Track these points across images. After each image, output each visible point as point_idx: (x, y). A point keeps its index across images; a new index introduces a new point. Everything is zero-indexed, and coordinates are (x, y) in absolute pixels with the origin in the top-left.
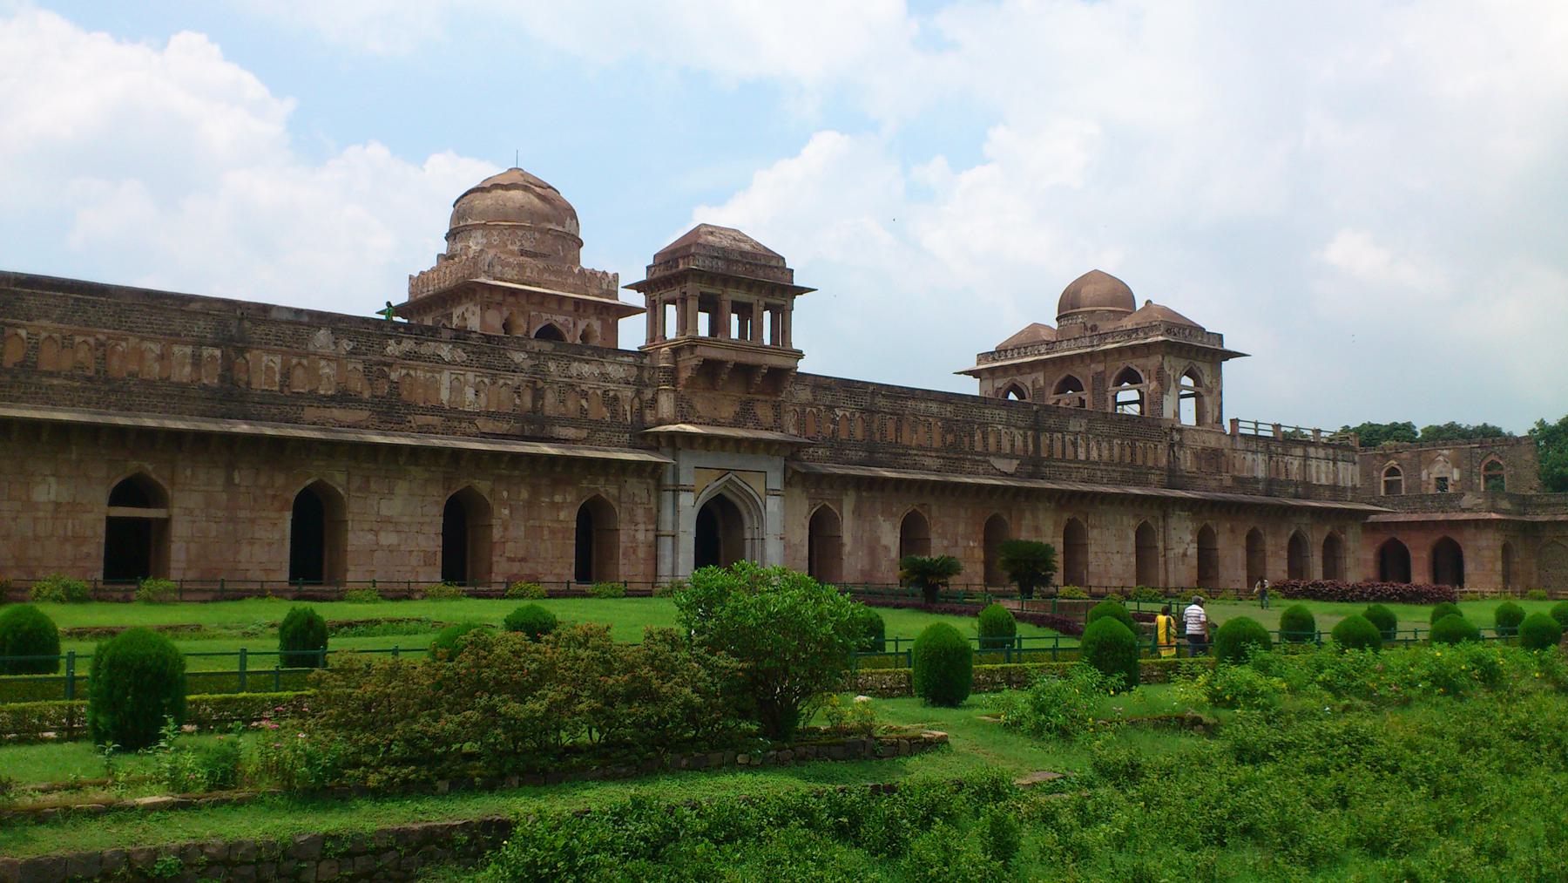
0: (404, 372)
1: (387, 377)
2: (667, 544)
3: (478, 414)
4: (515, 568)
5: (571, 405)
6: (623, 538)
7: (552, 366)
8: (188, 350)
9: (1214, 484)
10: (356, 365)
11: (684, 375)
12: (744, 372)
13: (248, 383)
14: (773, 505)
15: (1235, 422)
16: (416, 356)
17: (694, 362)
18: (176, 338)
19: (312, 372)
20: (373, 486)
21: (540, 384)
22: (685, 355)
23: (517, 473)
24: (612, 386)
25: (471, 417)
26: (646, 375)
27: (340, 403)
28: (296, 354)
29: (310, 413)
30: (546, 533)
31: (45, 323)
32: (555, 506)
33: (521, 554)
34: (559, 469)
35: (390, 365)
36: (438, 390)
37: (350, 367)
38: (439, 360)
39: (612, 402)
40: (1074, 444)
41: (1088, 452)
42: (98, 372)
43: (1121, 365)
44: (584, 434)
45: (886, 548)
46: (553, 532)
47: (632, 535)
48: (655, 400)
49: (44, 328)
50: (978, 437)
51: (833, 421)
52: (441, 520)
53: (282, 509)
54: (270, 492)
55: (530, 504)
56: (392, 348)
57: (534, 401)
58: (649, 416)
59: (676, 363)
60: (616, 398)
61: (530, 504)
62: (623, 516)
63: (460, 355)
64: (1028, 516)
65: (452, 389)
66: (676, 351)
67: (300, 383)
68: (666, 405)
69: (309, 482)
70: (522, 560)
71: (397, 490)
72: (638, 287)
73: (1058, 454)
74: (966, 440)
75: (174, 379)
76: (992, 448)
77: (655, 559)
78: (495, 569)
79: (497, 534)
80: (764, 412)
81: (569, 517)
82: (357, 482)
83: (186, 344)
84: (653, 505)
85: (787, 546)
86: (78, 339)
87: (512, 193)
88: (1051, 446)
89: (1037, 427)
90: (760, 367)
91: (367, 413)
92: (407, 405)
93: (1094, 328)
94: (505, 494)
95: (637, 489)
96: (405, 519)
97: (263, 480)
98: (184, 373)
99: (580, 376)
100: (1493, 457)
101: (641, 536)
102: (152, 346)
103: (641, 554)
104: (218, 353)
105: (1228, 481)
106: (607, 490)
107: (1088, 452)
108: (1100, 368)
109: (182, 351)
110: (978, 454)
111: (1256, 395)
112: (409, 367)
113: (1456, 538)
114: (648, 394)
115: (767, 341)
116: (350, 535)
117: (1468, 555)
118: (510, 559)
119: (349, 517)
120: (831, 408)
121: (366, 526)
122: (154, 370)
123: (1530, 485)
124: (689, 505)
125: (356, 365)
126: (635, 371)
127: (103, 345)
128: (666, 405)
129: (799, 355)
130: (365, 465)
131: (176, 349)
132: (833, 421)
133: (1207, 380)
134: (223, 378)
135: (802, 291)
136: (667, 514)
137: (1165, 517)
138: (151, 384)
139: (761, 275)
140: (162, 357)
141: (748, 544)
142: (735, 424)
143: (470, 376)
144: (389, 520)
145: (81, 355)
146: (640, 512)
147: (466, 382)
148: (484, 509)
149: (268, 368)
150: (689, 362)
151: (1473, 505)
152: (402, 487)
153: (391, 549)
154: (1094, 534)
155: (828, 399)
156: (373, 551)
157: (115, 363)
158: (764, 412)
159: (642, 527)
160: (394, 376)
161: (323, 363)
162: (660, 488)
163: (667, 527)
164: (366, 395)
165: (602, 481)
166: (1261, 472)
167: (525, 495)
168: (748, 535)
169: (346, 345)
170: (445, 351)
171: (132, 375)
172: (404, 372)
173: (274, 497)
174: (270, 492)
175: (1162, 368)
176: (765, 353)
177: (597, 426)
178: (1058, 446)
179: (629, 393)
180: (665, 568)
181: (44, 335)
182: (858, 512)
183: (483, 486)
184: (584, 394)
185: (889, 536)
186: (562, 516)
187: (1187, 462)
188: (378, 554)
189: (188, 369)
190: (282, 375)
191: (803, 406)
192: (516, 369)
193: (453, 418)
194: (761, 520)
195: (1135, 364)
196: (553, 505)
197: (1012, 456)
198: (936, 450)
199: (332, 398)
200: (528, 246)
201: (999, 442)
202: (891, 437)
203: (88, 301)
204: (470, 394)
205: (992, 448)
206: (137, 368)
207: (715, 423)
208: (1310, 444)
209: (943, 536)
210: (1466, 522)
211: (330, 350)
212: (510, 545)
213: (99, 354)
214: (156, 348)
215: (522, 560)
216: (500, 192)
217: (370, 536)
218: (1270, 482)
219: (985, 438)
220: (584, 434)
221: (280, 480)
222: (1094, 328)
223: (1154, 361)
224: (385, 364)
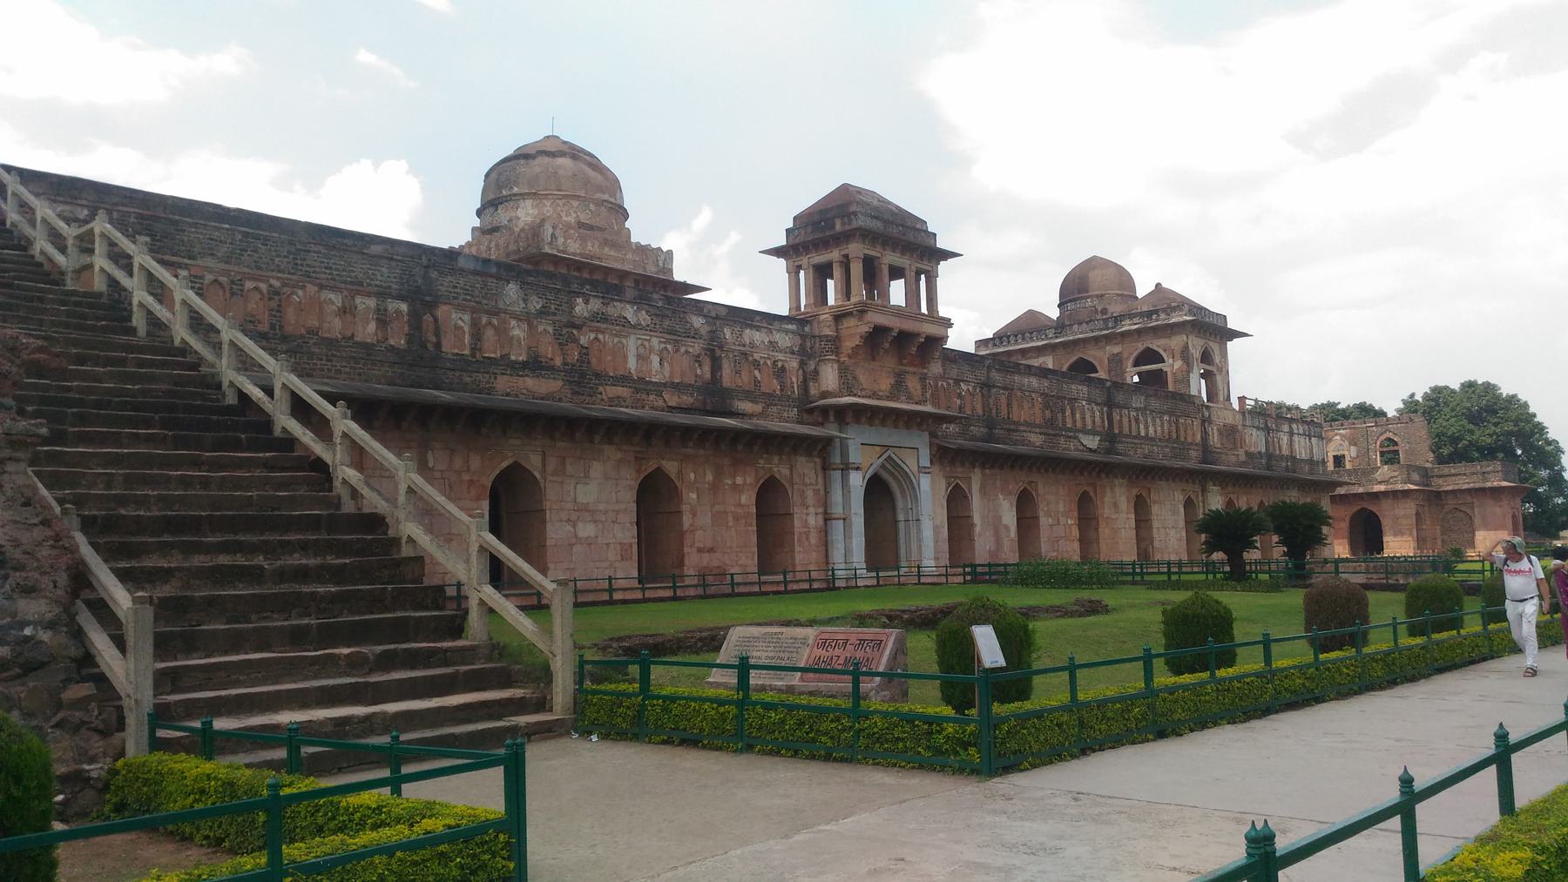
0: (592, 336)
1: (576, 341)
2: (838, 527)
3: (665, 385)
4: (706, 559)
5: (745, 376)
6: (797, 523)
7: (727, 332)
8: (372, 303)
9: (1233, 459)
10: (545, 326)
11: (848, 345)
12: (904, 338)
13: (438, 345)
14: (925, 483)
15: (1242, 399)
16: (605, 318)
17: (865, 329)
18: (357, 287)
19: (502, 331)
20: (569, 469)
21: (718, 352)
22: (850, 322)
23: (702, 452)
24: (781, 356)
25: (658, 388)
26: (808, 344)
27: (533, 371)
28: (488, 313)
29: (503, 383)
30: (730, 518)
31: (210, 262)
32: (736, 488)
33: (709, 544)
34: (740, 447)
35: (579, 327)
36: (625, 357)
37: (541, 328)
38: (625, 322)
39: (780, 372)
40: (1137, 420)
41: (1147, 428)
42: (272, 327)
44: (758, 408)
45: (1006, 527)
46: (736, 519)
47: (806, 519)
48: (816, 372)
49: (211, 271)
50: (1068, 413)
51: (959, 396)
52: (634, 506)
53: (478, 499)
54: (466, 477)
55: (715, 487)
56: (581, 308)
57: (713, 372)
58: (813, 391)
59: (837, 330)
60: (783, 369)
61: (715, 487)
62: (796, 498)
63: (645, 318)
64: (1108, 493)
65: (639, 357)
66: (839, 317)
67: (491, 350)
68: (829, 377)
69: (505, 464)
70: (711, 550)
71: (593, 473)
72: (777, 252)
73: (1126, 431)
74: (1060, 416)
75: (357, 339)
76: (1079, 425)
77: (826, 545)
78: (686, 562)
79: (687, 520)
80: (913, 384)
81: (748, 499)
82: (552, 464)
83: (369, 295)
84: (820, 486)
85: (936, 529)
86: (249, 285)
87: (560, 161)
88: (1120, 422)
89: (1110, 404)
90: (918, 335)
91: (560, 383)
92: (597, 375)
93: (1104, 311)
94: (692, 476)
95: (806, 468)
96: (601, 507)
97: (458, 463)
98: (368, 331)
99: (752, 345)
100: (1391, 435)
101: (812, 521)
102: (332, 296)
103: (813, 541)
104: (404, 307)
105: (1243, 458)
106: (781, 470)
107: (1147, 428)
108: (1116, 349)
109: (365, 303)
110: (1070, 430)
111: (1259, 373)
112: (598, 330)
113: (1374, 509)
114: (812, 365)
115: (924, 310)
116: (549, 526)
117: (1386, 523)
118: (700, 550)
119: (547, 505)
120: (957, 382)
121: (564, 516)
122: (335, 327)
123: (1427, 459)
124: (857, 481)
125: (545, 326)
126: (798, 340)
127: (278, 293)
128: (829, 377)
129: (947, 323)
130: (560, 444)
131: (358, 300)
132: (959, 396)
133: (1217, 359)
134: (410, 339)
135: (947, 255)
136: (837, 496)
137: (1204, 491)
138: (331, 343)
139: (910, 237)
140: (346, 311)
141: (902, 526)
142: (888, 398)
143: (655, 341)
144: (583, 509)
145: (251, 306)
146: (810, 493)
147: (651, 350)
148: (674, 493)
149: (457, 328)
150: (855, 330)
152: (597, 469)
153: (589, 543)
154: (1155, 509)
155: (954, 373)
156: (571, 545)
157: (290, 315)
159: (812, 510)
160: (583, 341)
161: (513, 323)
162: (826, 468)
163: (838, 510)
164: (558, 362)
165: (776, 459)
167: (709, 477)
168: (901, 517)
169: (536, 304)
170: (629, 312)
171: (313, 332)
172: (592, 336)
173: (471, 482)
174: (466, 477)
175: (1186, 347)
176: (923, 321)
177: (769, 399)
178: (1125, 420)
179: (793, 364)
180: (837, 556)
181: (209, 278)
182: (983, 489)
183: (671, 467)
184: (756, 364)
185: (1009, 517)
186: (744, 499)
187: (1215, 439)
188: (577, 548)
189: (372, 327)
190: (472, 335)
191: (936, 379)
192: (695, 335)
193: (641, 385)
194: (916, 498)
195: (1157, 344)
196: (735, 486)
197: (1093, 433)
198: (1039, 426)
199: (525, 365)
200: (584, 218)
201: (1083, 418)
202: (1004, 413)
203: (257, 238)
204: (655, 360)
205: (1079, 425)
206: (317, 324)
207: (874, 395)
208: (1292, 420)
209: (1048, 514)
210: (1385, 494)
211: (519, 307)
212: (699, 532)
213: (273, 304)
214: (336, 299)
215: (711, 550)
216: (547, 159)
217: (569, 528)
219: (1073, 414)
220: (758, 408)
221: (476, 462)
222: (1104, 311)
223: (1177, 341)
224: (574, 326)
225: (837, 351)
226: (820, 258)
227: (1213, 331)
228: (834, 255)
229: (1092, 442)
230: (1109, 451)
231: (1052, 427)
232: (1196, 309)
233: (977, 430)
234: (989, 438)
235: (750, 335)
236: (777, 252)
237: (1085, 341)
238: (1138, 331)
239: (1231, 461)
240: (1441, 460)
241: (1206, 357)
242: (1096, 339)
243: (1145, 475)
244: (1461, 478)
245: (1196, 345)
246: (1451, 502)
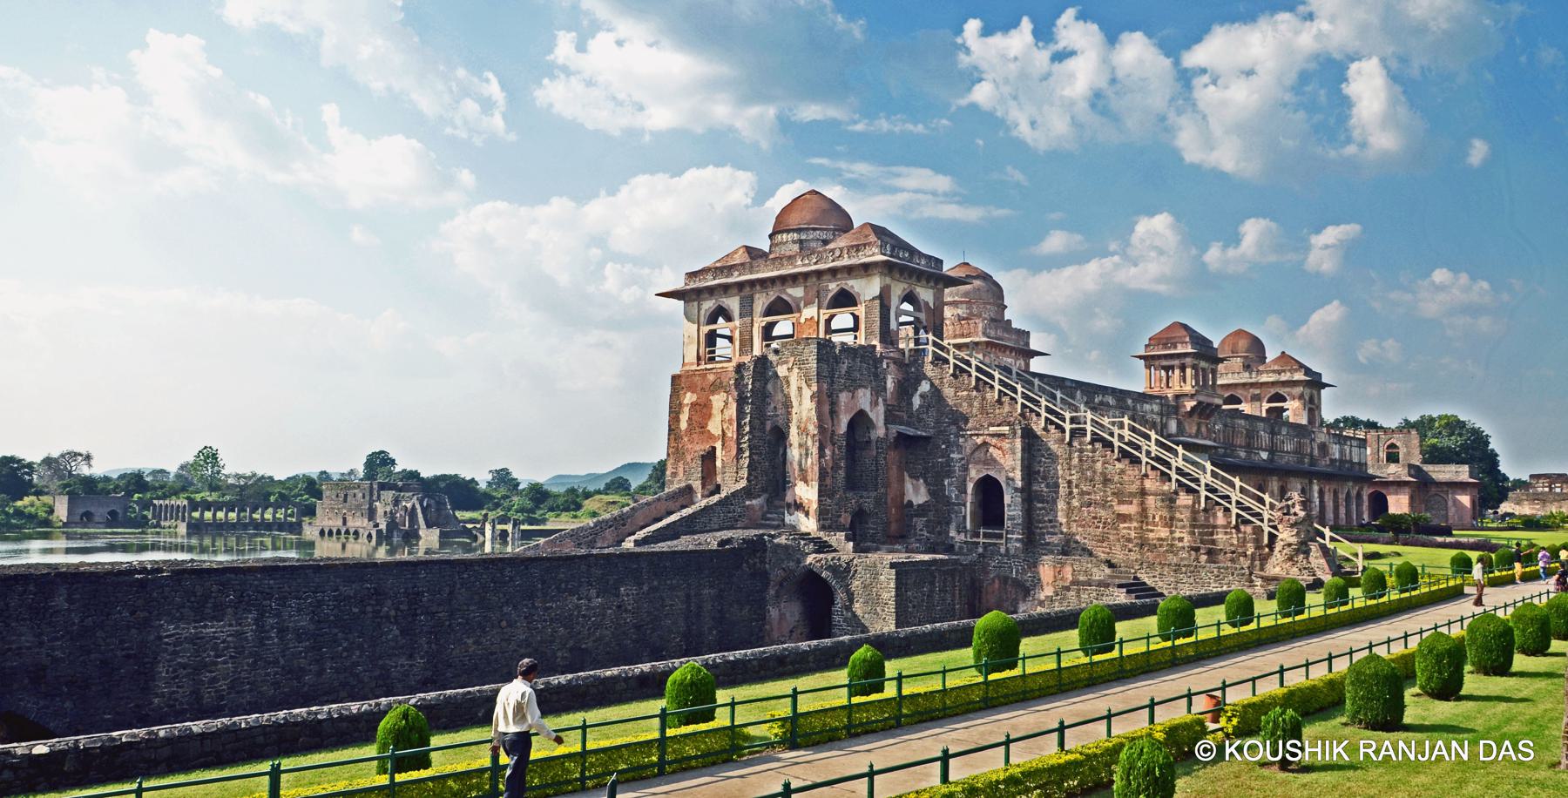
38: (1108, 405)
43: (1272, 391)
66: (1177, 397)
72: (1140, 357)
80: (1203, 429)
108: (1257, 391)
123: (1416, 460)
135: (1222, 360)
137: (1311, 483)
150: (1189, 405)
151: (1394, 471)
158: (1203, 429)
166: (1337, 456)
187: (1316, 452)
195: (1283, 391)
218: (1341, 461)
223: (1298, 390)
225: (1176, 413)
226: (1165, 363)
227: (1316, 383)
228: (1176, 362)
229: (1264, 455)
230: (1271, 460)
231: (1249, 447)
232: (1308, 371)
233: (1221, 451)
234: (1225, 455)
235: (1147, 407)
236: (1140, 357)
237: (1235, 386)
238: (1273, 384)
239: (1323, 465)
240: (1425, 462)
241: (1311, 400)
242: (1244, 385)
243: (1285, 473)
244: (1443, 473)
245: (1307, 391)
246: (1433, 490)
